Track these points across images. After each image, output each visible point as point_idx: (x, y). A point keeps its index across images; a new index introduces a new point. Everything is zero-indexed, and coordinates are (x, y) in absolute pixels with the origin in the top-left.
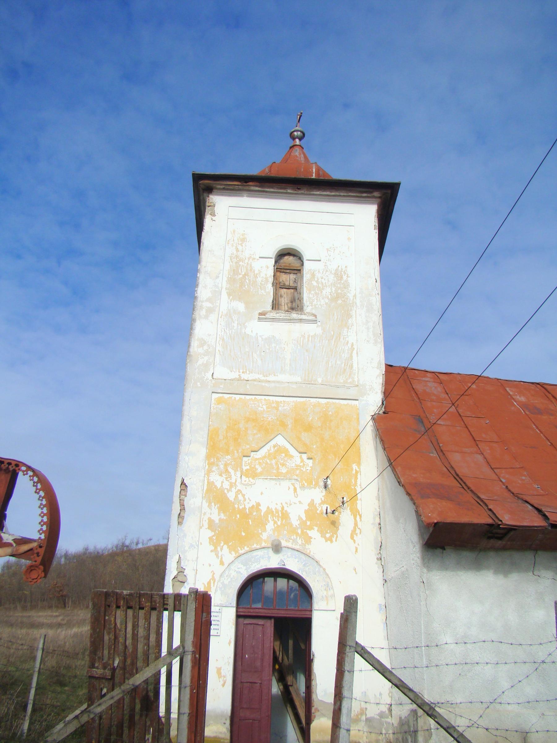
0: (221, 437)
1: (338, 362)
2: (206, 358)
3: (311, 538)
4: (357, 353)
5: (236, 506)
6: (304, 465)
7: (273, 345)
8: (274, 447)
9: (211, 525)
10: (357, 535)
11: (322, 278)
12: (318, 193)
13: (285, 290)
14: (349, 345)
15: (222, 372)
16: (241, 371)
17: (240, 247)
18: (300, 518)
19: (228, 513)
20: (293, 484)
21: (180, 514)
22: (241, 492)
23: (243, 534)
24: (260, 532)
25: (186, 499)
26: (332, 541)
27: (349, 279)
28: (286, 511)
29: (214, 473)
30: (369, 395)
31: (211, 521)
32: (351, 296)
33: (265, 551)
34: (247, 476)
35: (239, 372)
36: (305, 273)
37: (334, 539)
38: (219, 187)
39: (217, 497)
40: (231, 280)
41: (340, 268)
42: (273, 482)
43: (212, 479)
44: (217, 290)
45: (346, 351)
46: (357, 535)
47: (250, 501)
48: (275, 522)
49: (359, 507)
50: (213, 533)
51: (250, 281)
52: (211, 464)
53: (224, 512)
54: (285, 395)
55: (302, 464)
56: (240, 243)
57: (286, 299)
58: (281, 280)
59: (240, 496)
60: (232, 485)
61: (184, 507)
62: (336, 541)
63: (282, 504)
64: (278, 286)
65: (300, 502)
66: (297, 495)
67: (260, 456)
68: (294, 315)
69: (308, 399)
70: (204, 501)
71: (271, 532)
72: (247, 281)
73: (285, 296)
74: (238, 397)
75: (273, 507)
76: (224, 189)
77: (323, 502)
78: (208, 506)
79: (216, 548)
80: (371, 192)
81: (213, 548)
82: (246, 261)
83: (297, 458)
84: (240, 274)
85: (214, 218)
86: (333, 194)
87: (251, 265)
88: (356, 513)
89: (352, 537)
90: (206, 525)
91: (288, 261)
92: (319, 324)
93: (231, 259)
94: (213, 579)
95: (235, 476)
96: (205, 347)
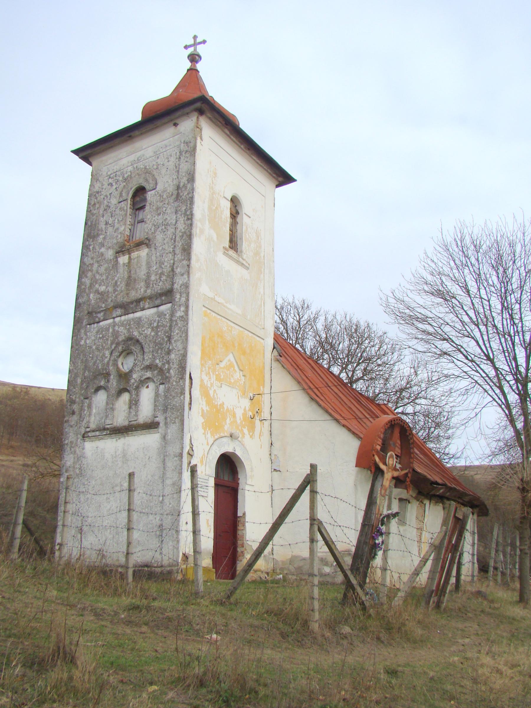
12: (255, 158)
18: (240, 419)
31: (203, 410)
38: (209, 115)
48: (230, 419)
52: (202, 365)
83: (238, 375)
94: (204, 455)
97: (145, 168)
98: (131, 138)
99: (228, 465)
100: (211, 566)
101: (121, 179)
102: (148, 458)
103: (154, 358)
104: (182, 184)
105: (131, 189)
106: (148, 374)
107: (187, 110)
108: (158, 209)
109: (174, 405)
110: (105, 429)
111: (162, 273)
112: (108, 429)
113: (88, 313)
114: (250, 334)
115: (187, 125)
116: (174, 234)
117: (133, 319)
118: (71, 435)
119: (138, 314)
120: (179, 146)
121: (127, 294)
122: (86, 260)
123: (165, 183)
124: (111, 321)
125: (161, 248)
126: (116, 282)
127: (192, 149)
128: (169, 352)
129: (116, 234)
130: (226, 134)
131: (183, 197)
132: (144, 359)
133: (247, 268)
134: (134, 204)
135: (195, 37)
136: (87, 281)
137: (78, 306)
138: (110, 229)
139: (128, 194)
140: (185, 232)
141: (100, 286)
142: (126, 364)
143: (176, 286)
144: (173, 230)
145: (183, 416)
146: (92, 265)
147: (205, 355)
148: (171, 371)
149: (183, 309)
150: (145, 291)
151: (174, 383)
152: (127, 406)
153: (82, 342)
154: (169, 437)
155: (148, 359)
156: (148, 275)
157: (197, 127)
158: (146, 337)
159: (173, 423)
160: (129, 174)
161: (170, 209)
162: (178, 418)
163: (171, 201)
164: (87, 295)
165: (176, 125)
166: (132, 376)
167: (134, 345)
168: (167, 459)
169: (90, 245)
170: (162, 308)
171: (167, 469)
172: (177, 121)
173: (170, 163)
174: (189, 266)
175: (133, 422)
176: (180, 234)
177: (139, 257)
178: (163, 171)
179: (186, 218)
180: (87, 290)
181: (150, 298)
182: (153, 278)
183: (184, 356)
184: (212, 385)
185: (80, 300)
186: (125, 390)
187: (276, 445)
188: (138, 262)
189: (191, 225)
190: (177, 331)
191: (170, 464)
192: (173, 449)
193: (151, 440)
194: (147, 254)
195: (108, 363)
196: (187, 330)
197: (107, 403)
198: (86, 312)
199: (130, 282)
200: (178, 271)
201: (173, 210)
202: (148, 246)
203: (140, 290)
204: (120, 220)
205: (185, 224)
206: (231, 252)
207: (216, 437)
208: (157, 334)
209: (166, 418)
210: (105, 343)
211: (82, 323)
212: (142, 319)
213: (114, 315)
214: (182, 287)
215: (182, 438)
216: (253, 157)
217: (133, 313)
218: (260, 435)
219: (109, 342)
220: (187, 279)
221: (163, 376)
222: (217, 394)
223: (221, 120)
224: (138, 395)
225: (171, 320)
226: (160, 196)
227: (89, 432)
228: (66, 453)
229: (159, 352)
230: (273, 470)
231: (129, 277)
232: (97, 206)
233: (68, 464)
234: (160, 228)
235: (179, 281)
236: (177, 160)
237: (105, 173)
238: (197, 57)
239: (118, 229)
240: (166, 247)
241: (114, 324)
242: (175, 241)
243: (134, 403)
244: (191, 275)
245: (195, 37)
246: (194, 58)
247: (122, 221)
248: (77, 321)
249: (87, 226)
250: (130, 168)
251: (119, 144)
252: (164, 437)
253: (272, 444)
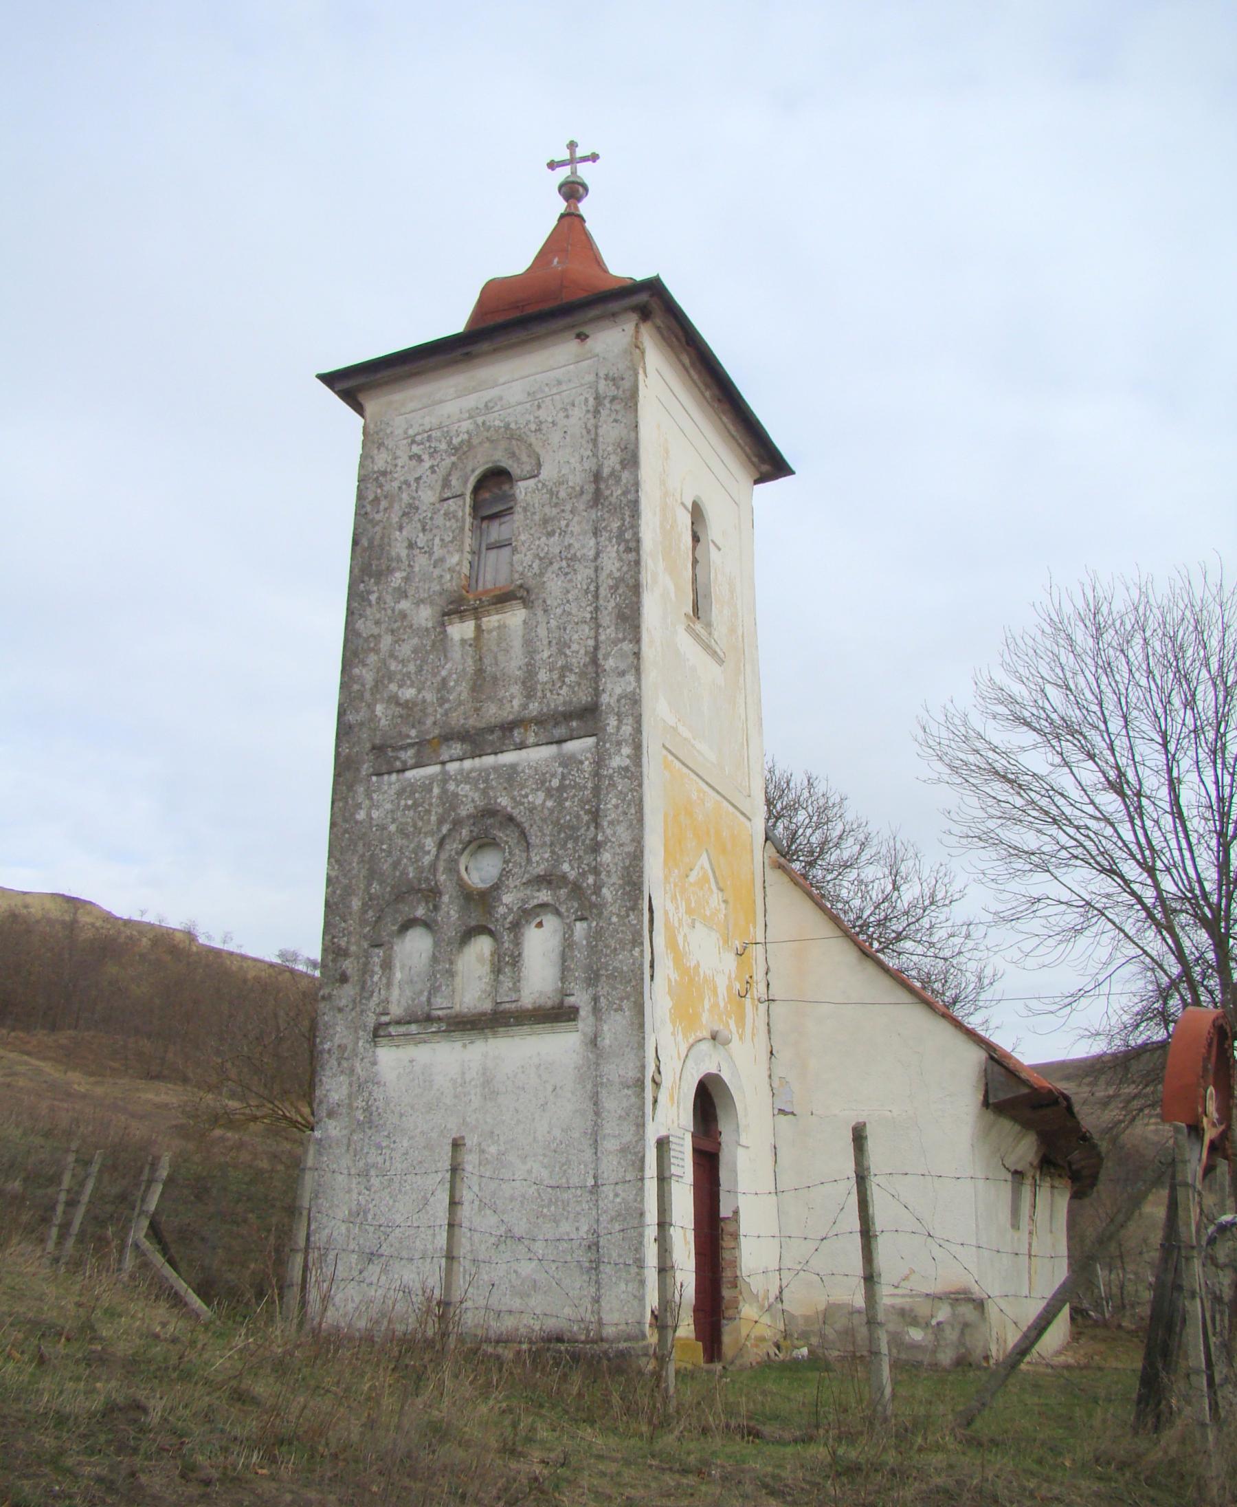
38: (659, 322)
83: (715, 899)
94: (674, 1082)
97: (507, 427)
98: (469, 357)
99: (709, 1101)
100: (693, 1335)
101: (443, 446)
102: (550, 1088)
103: (558, 861)
104: (606, 472)
105: (473, 471)
106: (544, 896)
107: (614, 306)
108: (545, 521)
109: (615, 969)
110: (429, 1019)
111: (566, 668)
112: (439, 1019)
113: (374, 748)
114: (731, 809)
115: (612, 339)
116: (595, 580)
117: (495, 769)
118: (339, 1031)
119: (508, 758)
120: (594, 386)
121: (477, 710)
122: (360, 625)
123: (562, 463)
124: (434, 769)
125: (559, 611)
126: (444, 681)
127: (628, 394)
128: (596, 848)
129: (437, 572)
130: (683, 365)
131: (613, 500)
132: (529, 860)
133: (720, 662)
134: (476, 508)
135: (572, 146)
136: (369, 676)
137: (344, 731)
138: (421, 561)
139: (466, 482)
140: (622, 579)
141: (400, 686)
142: (482, 870)
143: (605, 699)
144: (591, 572)
145: (642, 994)
146: (377, 638)
147: (671, 858)
148: (604, 890)
149: (626, 750)
150: (524, 706)
151: (614, 919)
152: (487, 968)
153: (361, 815)
154: (607, 1042)
155: (540, 862)
156: (530, 672)
157: (637, 347)
158: (532, 809)
159: (616, 1010)
160: (466, 437)
161: (579, 523)
162: (628, 998)
163: (582, 507)
164: (369, 706)
165: (582, 337)
166: (500, 899)
167: (502, 826)
168: (603, 1093)
169: (369, 592)
170: (571, 746)
171: (605, 1114)
172: (586, 330)
173: (573, 420)
174: (637, 655)
175: (507, 1006)
176: (611, 582)
177: (502, 627)
178: (555, 437)
179: (622, 548)
180: (367, 695)
181: (540, 721)
182: (543, 676)
183: (637, 857)
184: (680, 921)
185: (351, 718)
186: (483, 930)
187: (783, 1055)
188: (501, 639)
189: (637, 563)
190: (614, 801)
191: (612, 1104)
192: (618, 1070)
193: (559, 1047)
194: (525, 622)
195: (433, 867)
196: (641, 800)
197: (435, 959)
198: (368, 746)
199: (483, 682)
200: (610, 664)
201: (588, 527)
202: (526, 603)
203: (512, 702)
204: (447, 539)
205: (621, 560)
206: (698, 627)
207: (691, 1041)
208: (560, 803)
209: (596, 999)
210: (422, 819)
211: (358, 770)
212: (520, 769)
213: (445, 757)
214: (623, 701)
215: (641, 1045)
216: (724, 418)
217: (496, 754)
218: (753, 1034)
219: (433, 818)
220: (634, 684)
221: (583, 901)
223: (680, 334)
224: (517, 943)
225: (596, 774)
226: (551, 492)
227: (388, 1024)
228: (328, 1073)
229: (570, 845)
230: (776, 1112)
231: (480, 672)
232: (384, 504)
233: (335, 1097)
234: (556, 566)
235: (613, 690)
236: (590, 416)
237: (399, 432)
238: (581, 190)
239: (442, 560)
240: (573, 608)
241: (445, 778)
242: (596, 597)
243: (507, 962)
244: (643, 676)
245: (572, 146)
246: (573, 191)
247: (452, 542)
248: (345, 768)
249: (358, 548)
250: (467, 425)
251: (435, 369)
252: (593, 1041)
253: (771, 1053)
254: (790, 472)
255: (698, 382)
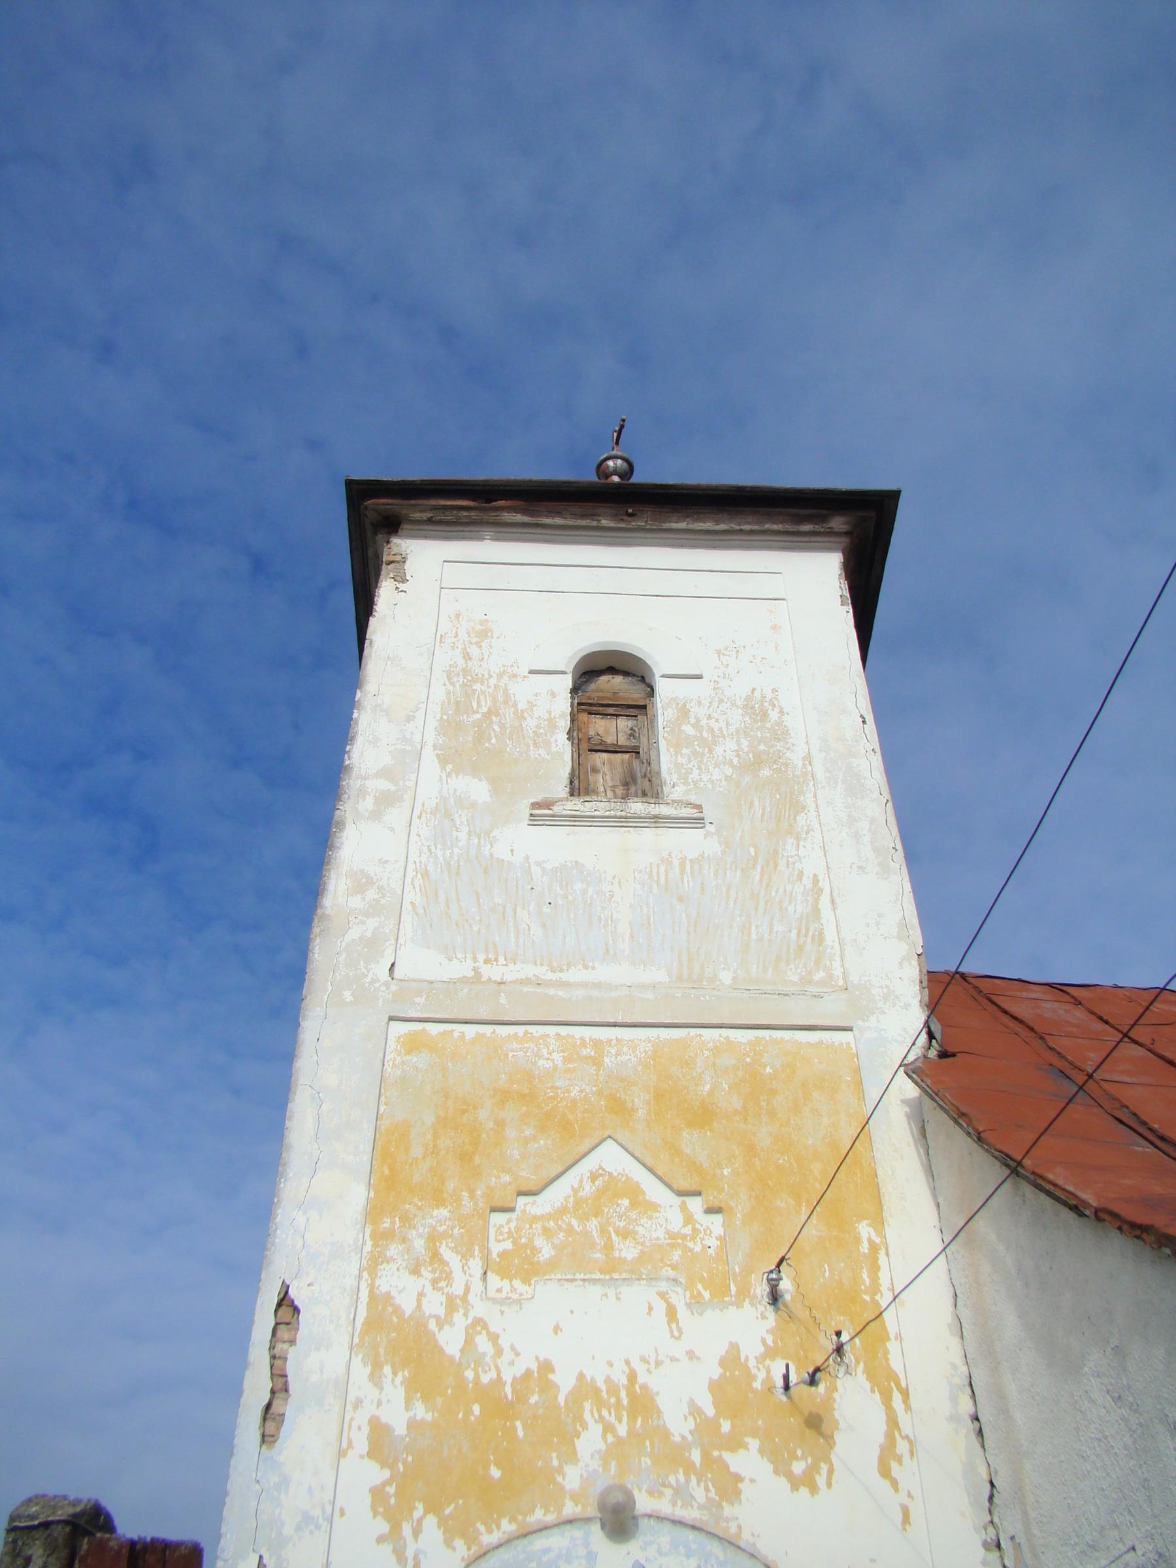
0: (417, 1151)
1: (778, 927)
2: (372, 923)
3: (738, 1478)
4: (833, 902)
5: (469, 1374)
6: (694, 1230)
7: (578, 886)
8: (594, 1177)
9: (380, 1441)
10: (899, 1460)
11: (709, 717)
12: (682, 525)
13: (605, 756)
14: (807, 881)
15: (421, 962)
16: (481, 957)
17: (474, 651)
18: (695, 1410)
19: (439, 1400)
20: (662, 1295)
21: (268, 1407)
22: (485, 1326)
23: (495, 1473)
24: (555, 1462)
25: (292, 1353)
26: (814, 1489)
27: (785, 718)
28: (644, 1387)
29: (393, 1266)
30: (883, 1013)
31: (379, 1432)
32: (796, 758)
33: (577, 1532)
34: (505, 1274)
35: (475, 960)
36: (659, 706)
37: (821, 1480)
38: (417, 515)
39: (398, 1342)
40: (450, 726)
41: (757, 694)
42: (595, 1290)
43: (383, 1285)
44: (408, 748)
45: (800, 897)
46: (899, 1460)
47: (518, 1354)
48: (608, 1428)
49: (896, 1363)
50: (386, 1474)
51: (503, 727)
52: (382, 1238)
53: (426, 1398)
54: (620, 1020)
55: (688, 1230)
56: (474, 640)
57: (608, 777)
58: (592, 733)
59: (483, 1343)
60: (451, 1305)
61: (286, 1383)
62: (829, 1485)
63: (627, 1362)
64: (585, 746)
65: (691, 1355)
66: (679, 1329)
67: (548, 1209)
68: (637, 807)
69: (693, 1031)
70: (357, 1361)
71: (595, 1464)
72: (496, 728)
73: (606, 769)
74: (470, 1030)
75: (598, 1374)
76: (430, 521)
77: (771, 1352)
78: (372, 1377)
79: (396, 1527)
80: (823, 519)
81: (383, 1527)
82: (493, 681)
83: (669, 1213)
84: (474, 712)
85: (402, 586)
86: (723, 527)
87: (506, 690)
88: (886, 1383)
89: (885, 1472)
90: (361, 1443)
91: (610, 686)
92: (710, 828)
93: (449, 678)
95: (464, 1272)
96: (371, 894)
216: (674, 525)
222: (494, 1338)
254: (893, 497)
255: (570, 522)
